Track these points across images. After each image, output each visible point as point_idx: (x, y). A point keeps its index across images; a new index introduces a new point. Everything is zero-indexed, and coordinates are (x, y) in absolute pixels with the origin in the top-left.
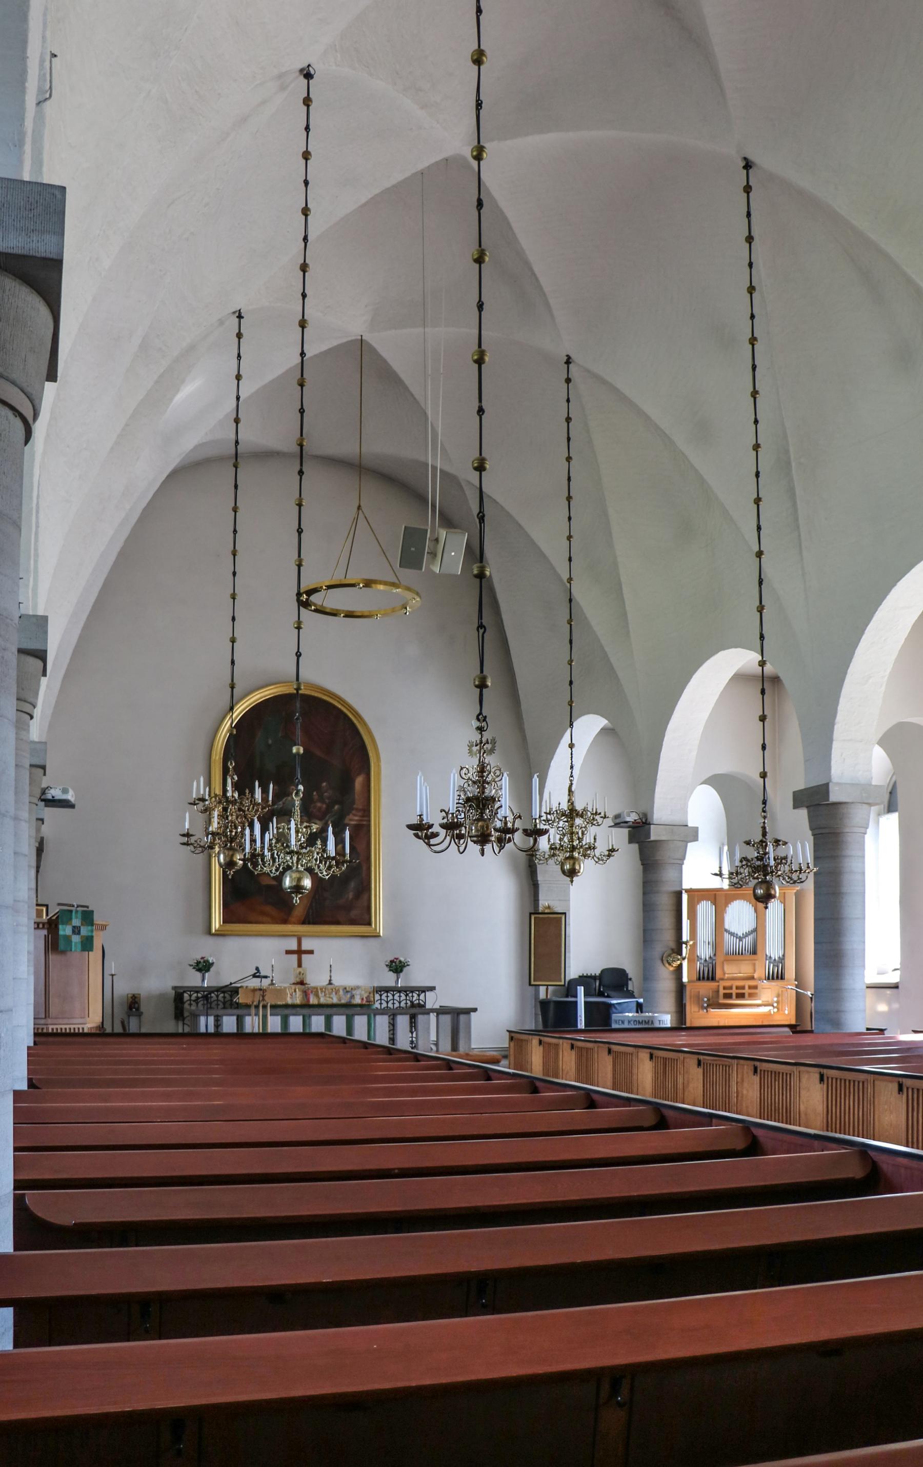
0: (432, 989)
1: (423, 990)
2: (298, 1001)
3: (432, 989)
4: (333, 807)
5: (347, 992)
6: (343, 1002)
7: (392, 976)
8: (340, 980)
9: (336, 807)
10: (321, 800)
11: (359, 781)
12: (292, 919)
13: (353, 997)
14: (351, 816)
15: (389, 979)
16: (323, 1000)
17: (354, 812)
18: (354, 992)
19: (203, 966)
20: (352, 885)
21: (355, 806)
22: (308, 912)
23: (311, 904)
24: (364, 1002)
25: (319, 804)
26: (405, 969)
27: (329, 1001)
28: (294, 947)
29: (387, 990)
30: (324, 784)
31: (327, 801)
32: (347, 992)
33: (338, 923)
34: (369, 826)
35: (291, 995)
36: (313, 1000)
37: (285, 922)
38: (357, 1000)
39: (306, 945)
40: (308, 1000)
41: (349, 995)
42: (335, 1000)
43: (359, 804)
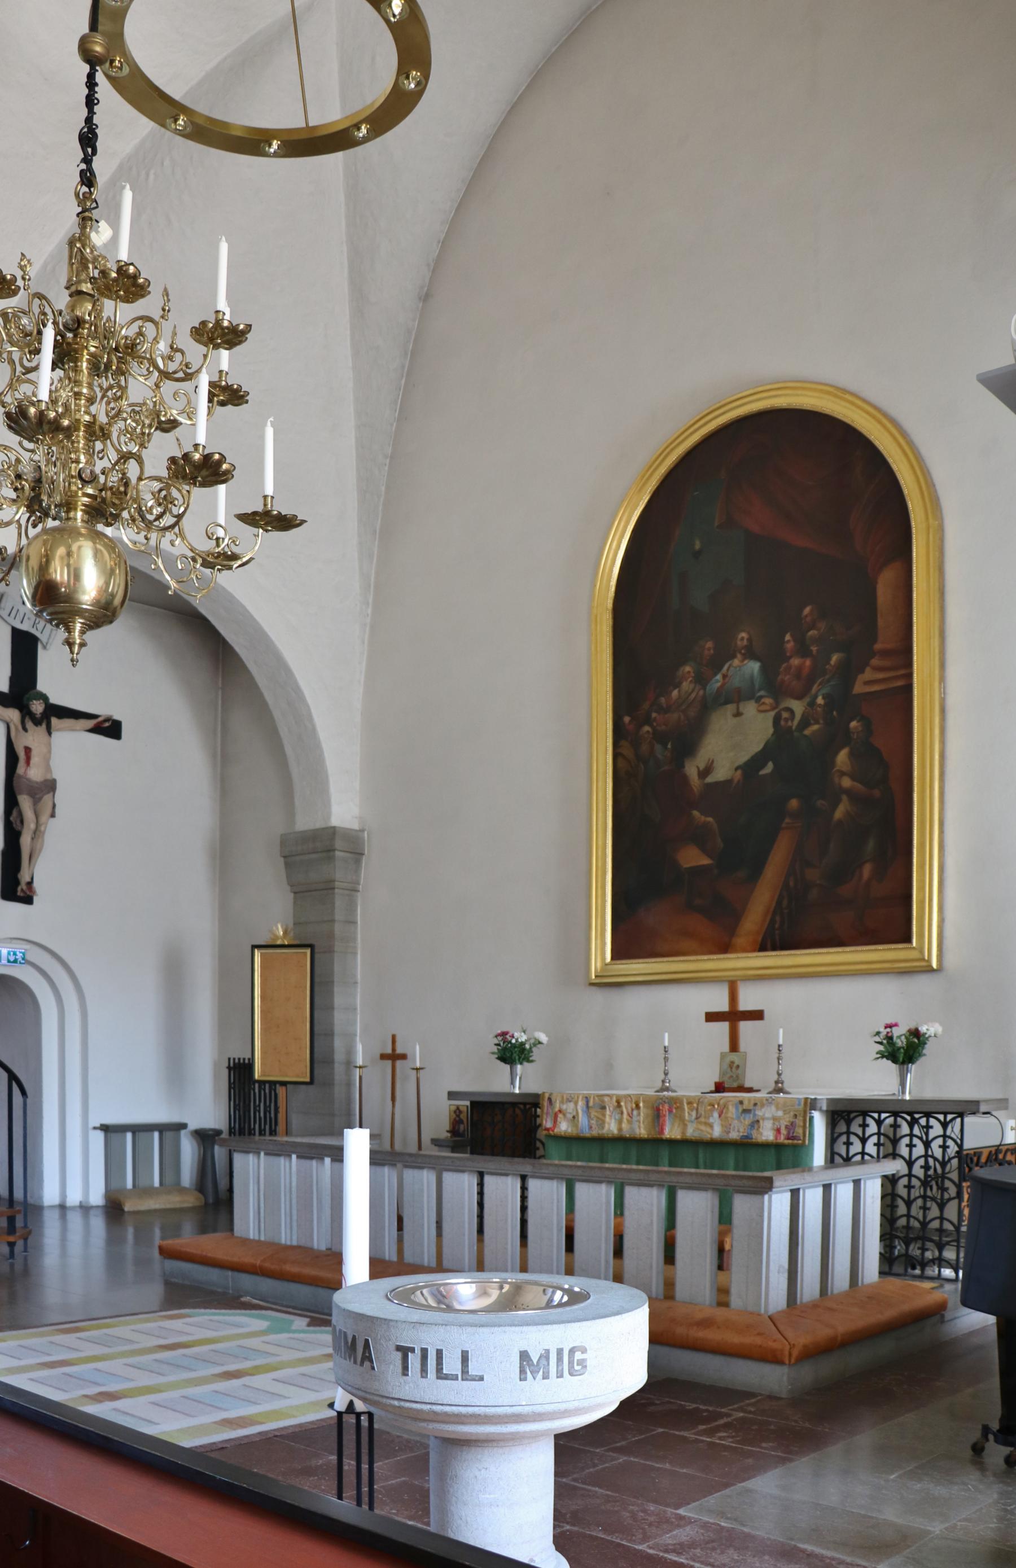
2: (642, 1131)
4: (830, 659)
5: (746, 1111)
6: (734, 1136)
9: (835, 658)
10: (803, 650)
12: (740, 941)
13: (756, 1123)
14: (868, 674)
17: (875, 662)
18: (759, 1113)
21: (878, 646)
22: (772, 922)
23: (779, 903)
24: (782, 1139)
25: (796, 662)
28: (722, 1005)
30: (807, 610)
31: (814, 649)
32: (746, 1111)
35: (630, 1116)
36: (671, 1131)
38: (767, 1134)
39: (749, 999)
40: (662, 1131)
41: (748, 1119)
42: (717, 1132)
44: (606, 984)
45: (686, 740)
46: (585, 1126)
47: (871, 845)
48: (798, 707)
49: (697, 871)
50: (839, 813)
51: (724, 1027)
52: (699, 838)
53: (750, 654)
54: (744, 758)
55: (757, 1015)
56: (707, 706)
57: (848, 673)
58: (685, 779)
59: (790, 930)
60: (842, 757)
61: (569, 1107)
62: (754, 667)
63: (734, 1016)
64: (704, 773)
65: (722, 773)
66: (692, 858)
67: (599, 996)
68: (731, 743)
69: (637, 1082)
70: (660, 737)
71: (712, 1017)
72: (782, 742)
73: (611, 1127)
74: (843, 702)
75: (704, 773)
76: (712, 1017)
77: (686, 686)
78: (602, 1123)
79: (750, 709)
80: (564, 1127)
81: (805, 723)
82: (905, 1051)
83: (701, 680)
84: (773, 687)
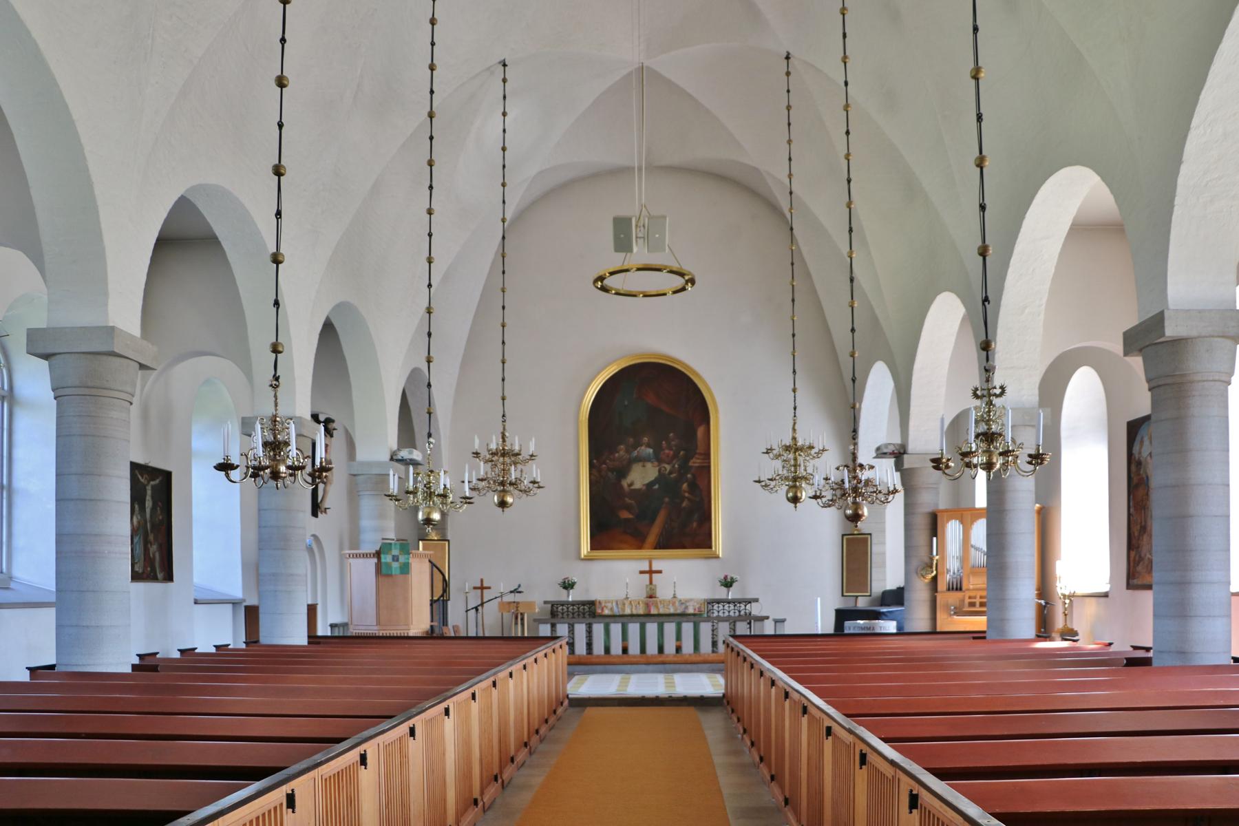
0: (756, 600)
1: (749, 602)
2: (641, 612)
3: (756, 600)
7: (725, 589)
8: (680, 596)
11: (700, 431)
13: (686, 607)
15: (722, 593)
16: (662, 611)
19: (568, 585)
20: (696, 516)
26: (735, 585)
27: (667, 612)
29: (718, 601)
33: (684, 547)
34: (709, 467)
36: (654, 611)
37: (640, 547)
38: (691, 611)
42: (672, 611)
43: (701, 449)
44: (587, 559)
45: (623, 472)
46: (616, 611)
47: (696, 516)
48: (668, 467)
49: (627, 520)
50: (684, 504)
51: (647, 576)
52: (628, 508)
53: (648, 446)
54: (646, 482)
55: (660, 572)
56: (631, 462)
57: (687, 459)
58: (622, 487)
59: (668, 542)
60: (685, 486)
61: (609, 605)
62: (651, 451)
63: (651, 572)
64: (631, 484)
65: (638, 485)
66: (625, 515)
67: (582, 564)
68: (641, 476)
69: (621, 595)
70: (611, 470)
71: (642, 572)
72: (661, 478)
73: (628, 611)
74: (684, 467)
75: (631, 484)
76: (642, 572)
77: (622, 453)
78: (623, 610)
79: (649, 465)
80: (606, 612)
81: (670, 473)
82: (728, 583)
83: (628, 451)
84: (658, 458)
